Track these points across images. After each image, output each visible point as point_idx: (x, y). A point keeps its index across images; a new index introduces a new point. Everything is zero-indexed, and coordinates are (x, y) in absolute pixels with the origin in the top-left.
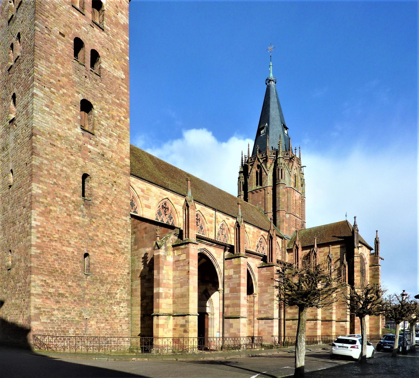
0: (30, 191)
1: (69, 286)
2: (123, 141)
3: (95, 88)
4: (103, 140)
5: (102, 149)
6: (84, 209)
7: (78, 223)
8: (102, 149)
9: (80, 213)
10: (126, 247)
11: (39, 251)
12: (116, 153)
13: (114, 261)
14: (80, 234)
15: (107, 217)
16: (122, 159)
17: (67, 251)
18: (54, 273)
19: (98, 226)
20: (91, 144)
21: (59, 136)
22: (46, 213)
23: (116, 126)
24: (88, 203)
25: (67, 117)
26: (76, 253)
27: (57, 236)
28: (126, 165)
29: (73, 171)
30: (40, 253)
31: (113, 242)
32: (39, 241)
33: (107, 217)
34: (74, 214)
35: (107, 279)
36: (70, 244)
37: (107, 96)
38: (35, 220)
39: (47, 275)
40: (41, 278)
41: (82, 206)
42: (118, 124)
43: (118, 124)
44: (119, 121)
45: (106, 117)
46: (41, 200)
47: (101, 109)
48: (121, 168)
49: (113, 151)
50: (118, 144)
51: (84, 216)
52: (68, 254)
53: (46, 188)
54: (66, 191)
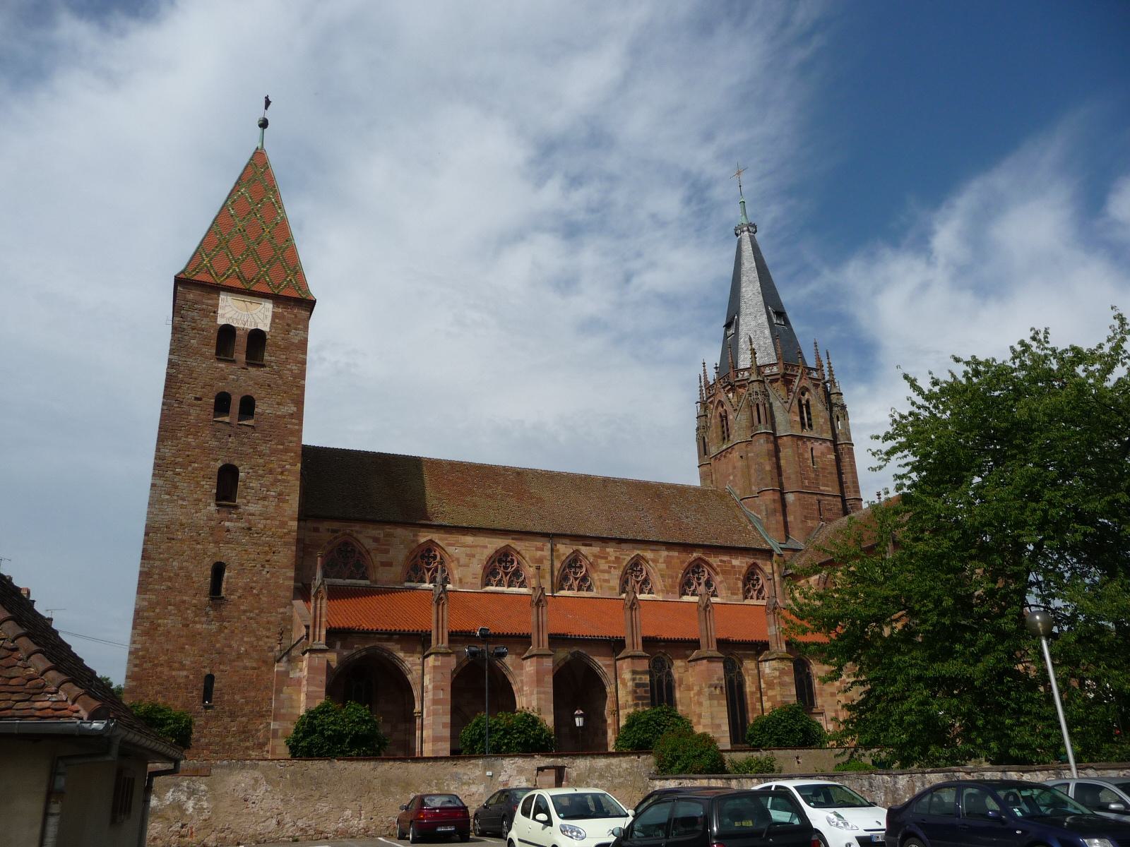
4: (252, 508)
5: (246, 522)
7: (200, 634)
9: (204, 619)
11: (134, 683)
12: (273, 518)
16: (283, 524)
19: (233, 632)
28: (288, 533)
31: (257, 651)
34: (195, 622)
37: (263, 448)
41: (208, 609)
42: (280, 477)
43: (280, 477)
44: (282, 473)
51: (209, 623)
53: (154, 597)
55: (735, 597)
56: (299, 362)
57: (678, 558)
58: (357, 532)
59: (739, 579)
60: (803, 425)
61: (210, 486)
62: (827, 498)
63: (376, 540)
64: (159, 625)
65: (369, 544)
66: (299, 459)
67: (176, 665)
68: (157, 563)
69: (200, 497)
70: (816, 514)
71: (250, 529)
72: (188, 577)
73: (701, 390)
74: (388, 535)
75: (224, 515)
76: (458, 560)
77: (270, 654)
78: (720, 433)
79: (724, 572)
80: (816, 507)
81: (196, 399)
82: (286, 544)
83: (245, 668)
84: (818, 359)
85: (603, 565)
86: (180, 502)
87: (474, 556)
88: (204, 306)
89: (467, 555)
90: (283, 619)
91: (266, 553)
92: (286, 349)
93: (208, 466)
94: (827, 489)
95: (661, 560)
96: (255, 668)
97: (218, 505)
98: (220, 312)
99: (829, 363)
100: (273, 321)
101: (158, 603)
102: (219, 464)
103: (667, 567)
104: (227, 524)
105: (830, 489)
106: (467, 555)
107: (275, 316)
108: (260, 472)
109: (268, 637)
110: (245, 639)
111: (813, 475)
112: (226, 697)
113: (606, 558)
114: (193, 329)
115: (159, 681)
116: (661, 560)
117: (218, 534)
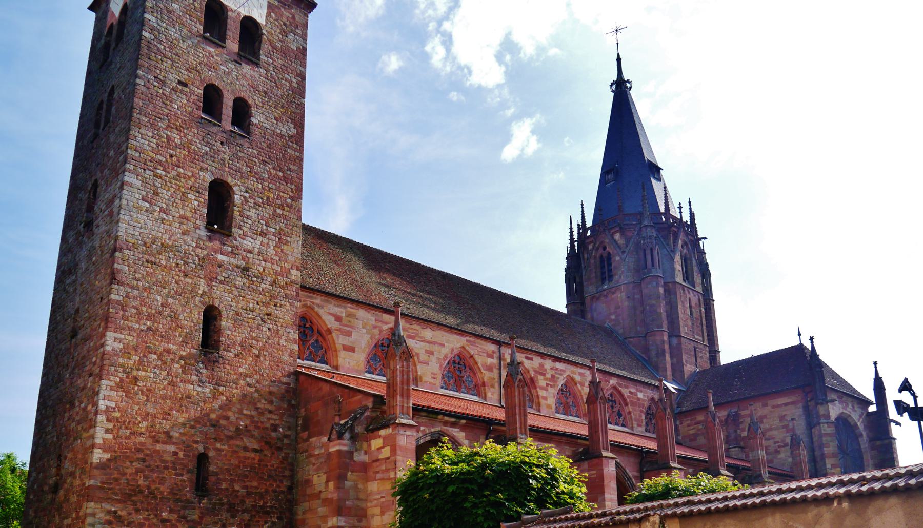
0: (103, 345)
2: (289, 239)
3: (239, 159)
4: (248, 243)
5: (243, 259)
6: (204, 371)
10: (286, 436)
13: (259, 465)
17: (164, 451)
18: (135, 495)
22: (127, 385)
25: (182, 212)
26: (181, 454)
27: (145, 424)
30: (108, 460)
31: (259, 428)
32: (110, 436)
36: (171, 437)
39: (119, 501)
40: (107, 506)
42: (279, 211)
44: (281, 207)
46: (121, 361)
47: (246, 192)
48: (282, 287)
51: (201, 383)
54: (168, 341)
58: (318, 306)
59: (641, 411)
63: (338, 319)
64: (136, 379)
65: (330, 322)
68: (136, 292)
71: (246, 269)
72: (174, 317)
73: (571, 232)
74: (349, 315)
75: (216, 244)
76: (418, 354)
77: (273, 434)
78: (599, 274)
83: (245, 449)
87: (432, 353)
89: (426, 351)
101: (135, 349)
106: (426, 351)
109: (270, 412)
110: (245, 412)
112: (224, 486)
113: (544, 375)
115: (141, 456)
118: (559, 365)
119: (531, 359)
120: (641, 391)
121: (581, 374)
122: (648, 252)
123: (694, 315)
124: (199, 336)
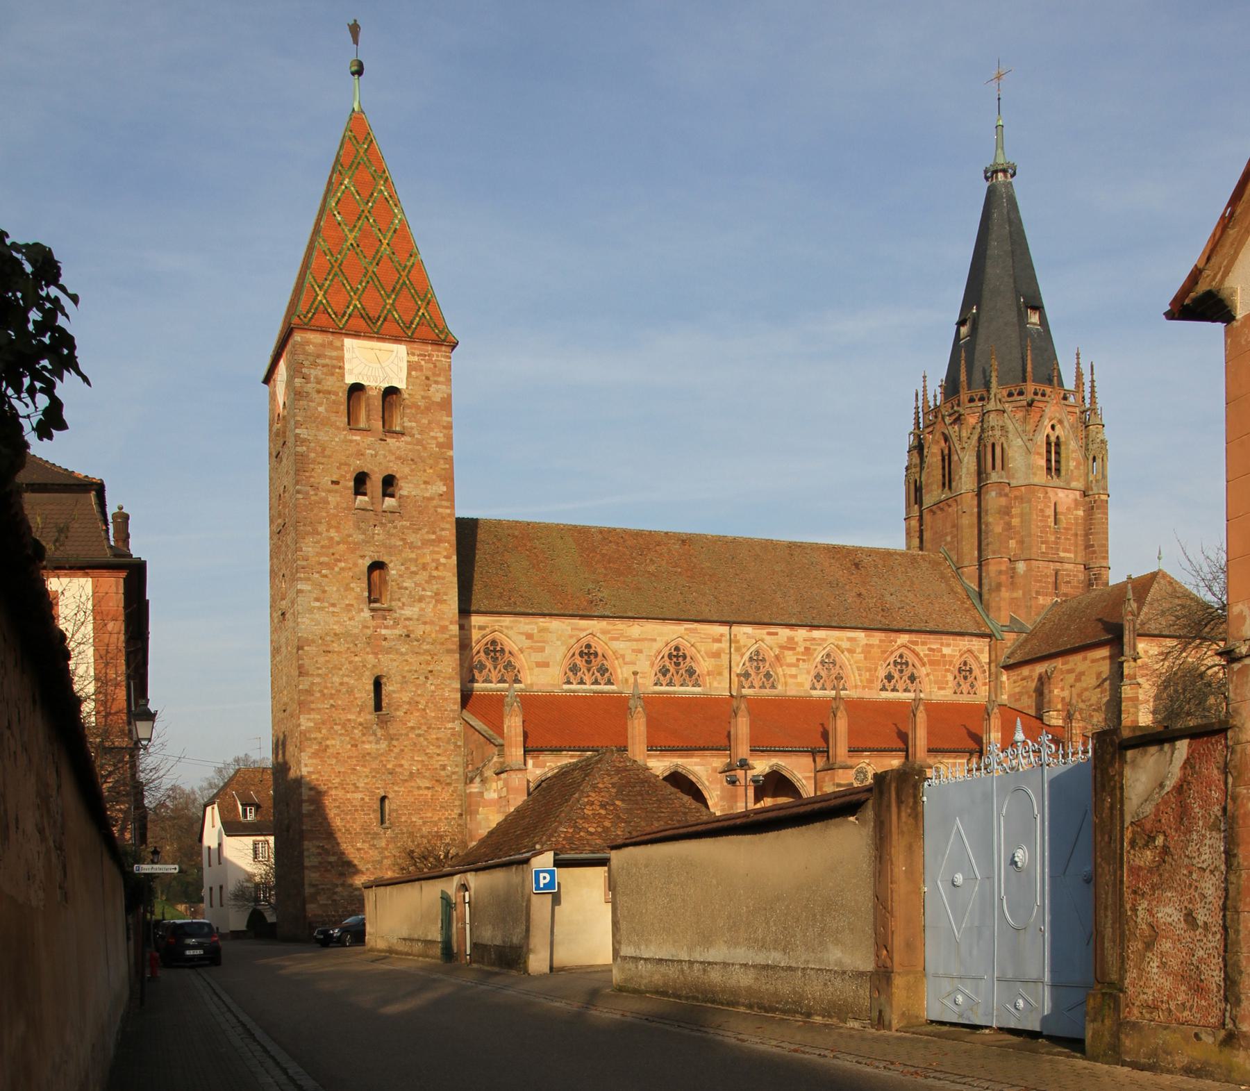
0: (299, 725)
1: (359, 850)
4: (407, 612)
5: (405, 627)
8: (405, 627)
9: (372, 738)
12: (432, 623)
14: (372, 770)
15: (417, 732)
16: (444, 629)
20: (386, 627)
21: (335, 634)
23: (432, 577)
24: (383, 722)
26: (367, 799)
27: (337, 780)
29: (359, 679)
33: (417, 732)
35: (420, 829)
37: (412, 538)
38: (306, 765)
41: (375, 727)
42: (435, 573)
43: (435, 573)
44: (437, 568)
45: (412, 573)
48: (442, 644)
49: (425, 623)
50: (435, 606)
51: (377, 742)
52: (355, 803)
55: (942, 692)
56: (445, 427)
57: (879, 647)
60: (1049, 469)
61: (360, 588)
62: (1067, 566)
64: (327, 746)
66: (453, 551)
67: (352, 788)
68: (317, 680)
69: (353, 602)
70: (1051, 587)
71: (408, 636)
77: (443, 773)
79: (932, 663)
80: (1051, 580)
81: (335, 483)
82: (449, 651)
83: (419, 788)
84: (1079, 376)
85: (790, 657)
86: (331, 609)
88: (327, 361)
90: (453, 735)
91: (428, 663)
92: (428, 409)
93: (355, 565)
94: (1068, 555)
95: (859, 650)
96: (428, 788)
97: (373, 610)
98: (347, 366)
99: (1093, 381)
100: (409, 374)
101: (323, 723)
102: (368, 562)
103: (865, 658)
104: (384, 632)
105: (1072, 555)
107: (411, 367)
108: (413, 569)
111: (1052, 538)
114: (319, 392)
116: (859, 650)
117: (375, 643)
118: (817, 634)
119: (776, 634)
120: (948, 645)
121: (850, 639)
122: (989, 449)
123: (1063, 524)
124: (372, 703)
